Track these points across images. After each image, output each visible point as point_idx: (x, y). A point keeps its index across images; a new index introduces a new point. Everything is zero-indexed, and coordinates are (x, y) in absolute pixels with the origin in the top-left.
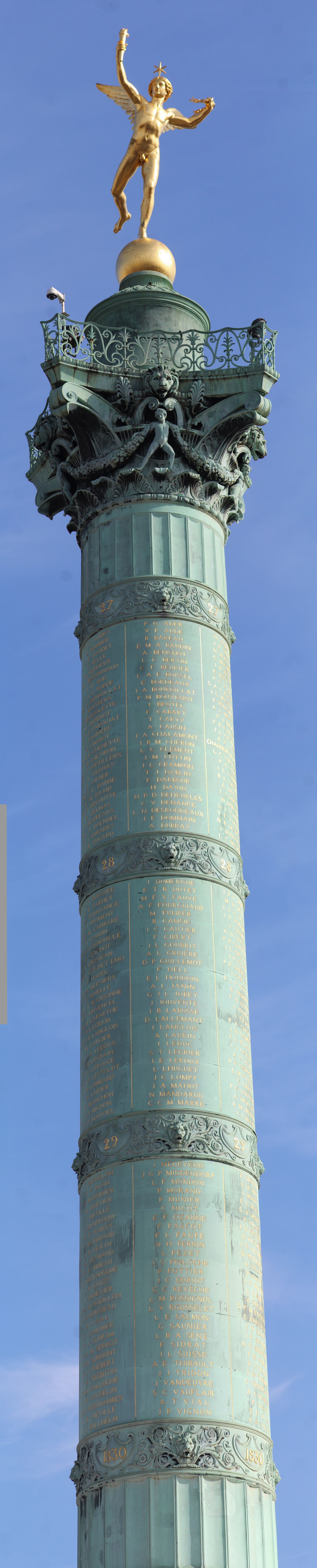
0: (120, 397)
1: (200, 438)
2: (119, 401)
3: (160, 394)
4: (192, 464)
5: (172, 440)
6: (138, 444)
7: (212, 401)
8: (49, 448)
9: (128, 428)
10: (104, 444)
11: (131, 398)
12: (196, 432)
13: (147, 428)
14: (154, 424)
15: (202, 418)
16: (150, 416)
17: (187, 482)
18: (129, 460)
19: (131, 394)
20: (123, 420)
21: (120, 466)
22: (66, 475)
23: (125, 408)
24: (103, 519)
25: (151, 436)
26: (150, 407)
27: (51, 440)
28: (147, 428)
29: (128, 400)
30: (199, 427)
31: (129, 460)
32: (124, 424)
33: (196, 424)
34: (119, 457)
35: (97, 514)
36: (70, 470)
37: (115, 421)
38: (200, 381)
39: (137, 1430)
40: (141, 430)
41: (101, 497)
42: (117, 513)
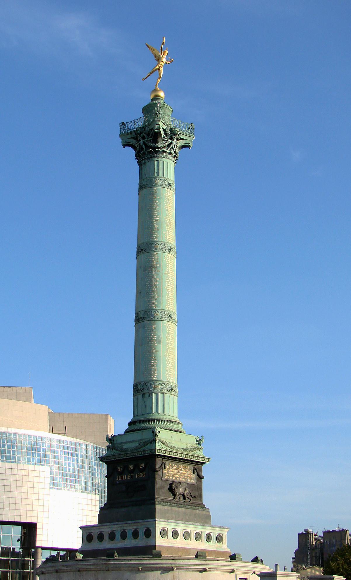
3: (175, 134)
7: (181, 139)
10: (160, 141)
13: (170, 141)
15: (178, 142)
17: (175, 156)
21: (163, 148)
22: (144, 143)
23: (165, 134)
24: (156, 159)
25: (171, 143)
27: (141, 133)
28: (170, 141)
35: (154, 157)
41: (156, 154)
42: (160, 159)
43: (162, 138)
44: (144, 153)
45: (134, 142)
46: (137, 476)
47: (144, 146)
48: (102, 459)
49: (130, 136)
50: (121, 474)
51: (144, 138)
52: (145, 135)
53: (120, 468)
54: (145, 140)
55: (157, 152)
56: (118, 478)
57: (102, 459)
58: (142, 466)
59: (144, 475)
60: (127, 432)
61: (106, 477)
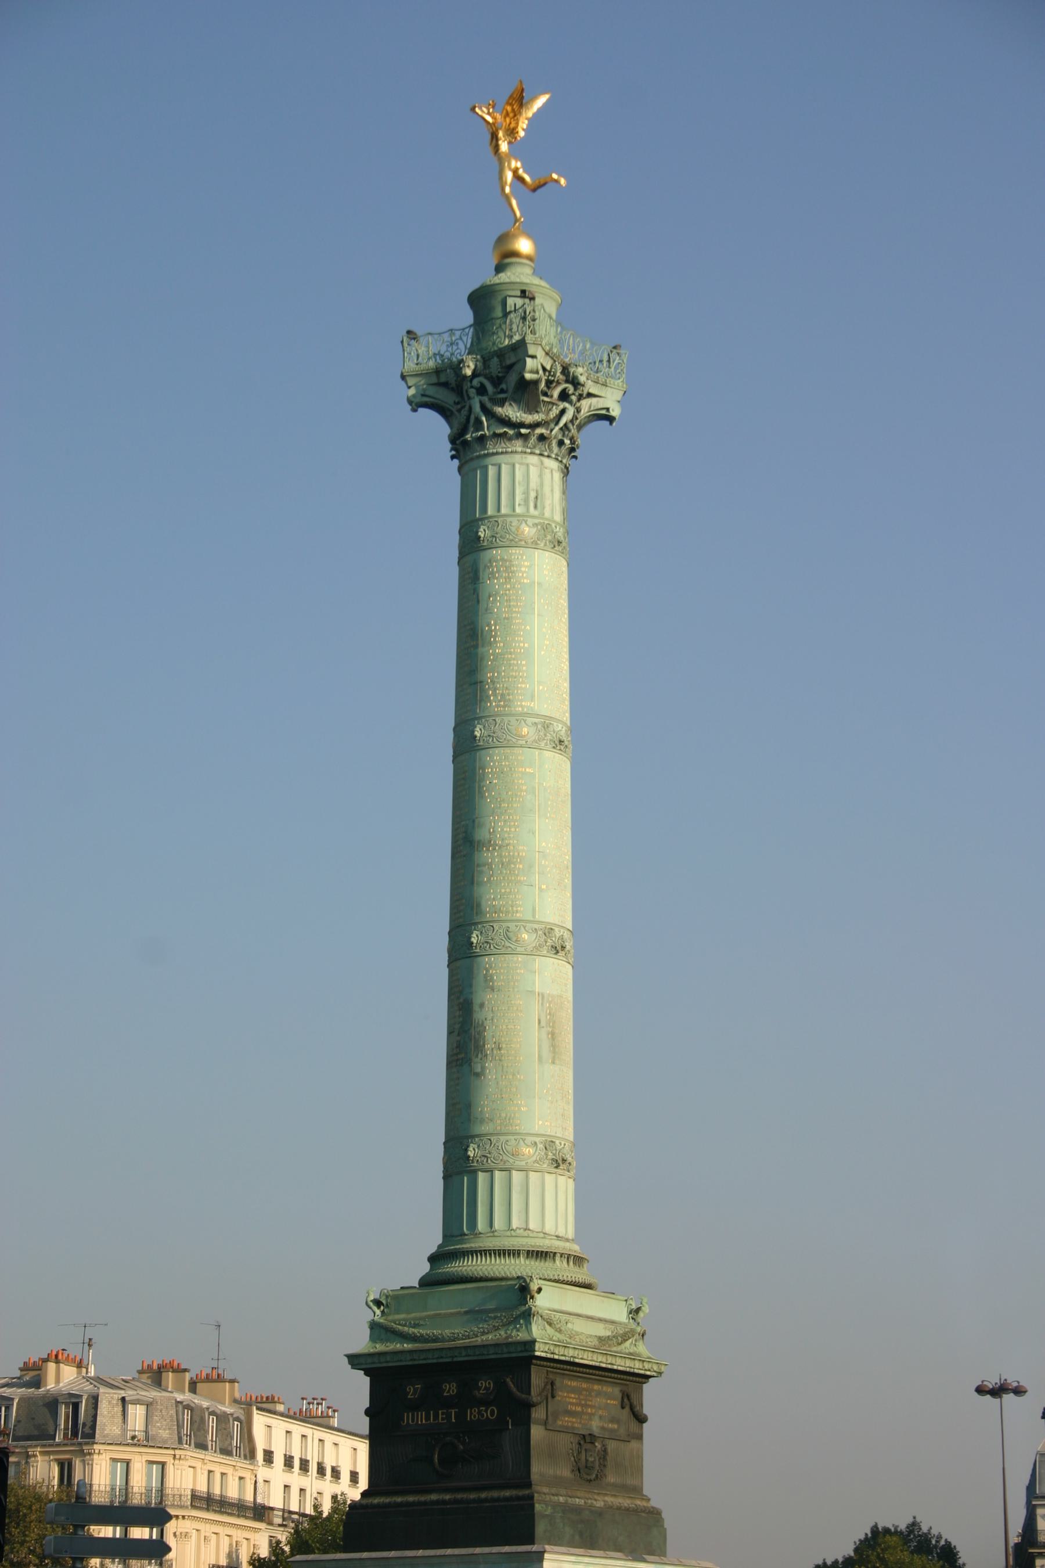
7: (590, 395)
13: (561, 407)
14: (567, 405)
16: (564, 396)
25: (563, 412)
36: (489, 405)
39: (537, 1140)
44: (482, 439)
45: (448, 398)
46: (472, 1414)
48: (355, 1360)
49: (434, 380)
50: (414, 1407)
51: (482, 391)
53: (412, 1391)
54: (485, 399)
56: (408, 1418)
57: (355, 1360)
58: (485, 1385)
59: (490, 1413)
60: (426, 1282)
61: (367, 1412)
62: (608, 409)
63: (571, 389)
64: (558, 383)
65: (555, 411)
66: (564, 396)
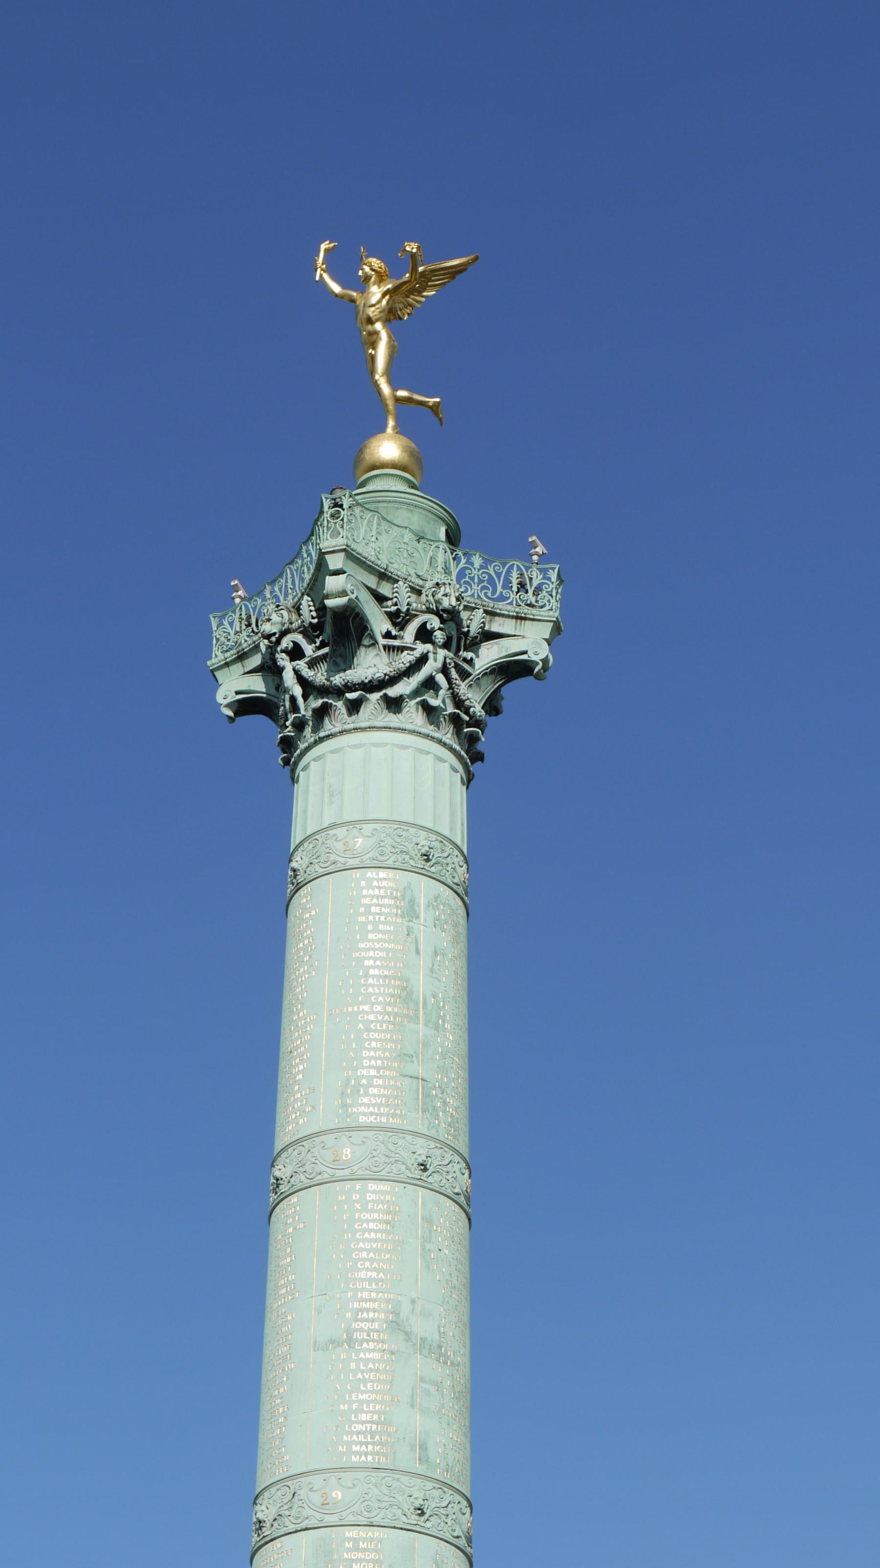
0: (396, 604)
1: (469, 675)
2: (394, 609)
4: (458, 702)
5: (445, 670)
6: (408, 665)
8: (278, 642)
9: (396, 643)
11: (408, 610)
12: (466, 666)
14: (429, 647)
16: (424, 634)
18: (392, 680)
19: (408, 604)
20: (394, 633)
25: (423, 659)
26: (429, 626)
28: (422, 648)
29: (404, 609)
30: (470, 662)
31: (392, 680)
32: (395, 637)
33: (469, 658)
34: (385, 675)
36: (307, 673)
37: (384, 631)
38: (481, 611)
40: (413, 649)
43: (375, 644)
47: (298, 691)
51: (296, 653)
52: (300, 638)
54: (301, 664)
55: (354, 707)
62: (525, 653)
63: (434, 622)
64: (409, 616)
65: (406, 659)
66: (424, 634)
